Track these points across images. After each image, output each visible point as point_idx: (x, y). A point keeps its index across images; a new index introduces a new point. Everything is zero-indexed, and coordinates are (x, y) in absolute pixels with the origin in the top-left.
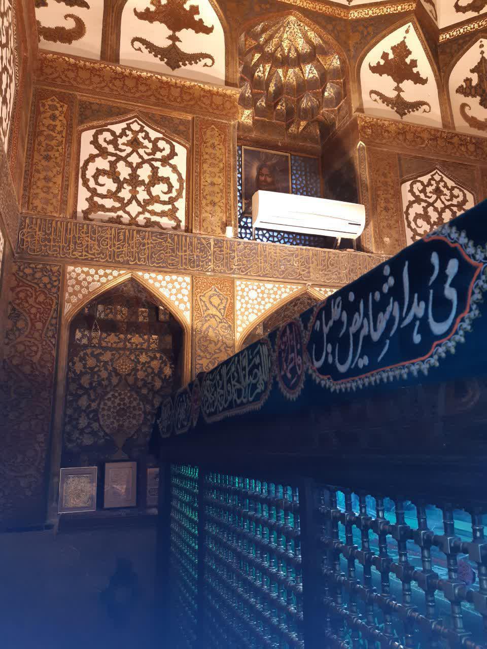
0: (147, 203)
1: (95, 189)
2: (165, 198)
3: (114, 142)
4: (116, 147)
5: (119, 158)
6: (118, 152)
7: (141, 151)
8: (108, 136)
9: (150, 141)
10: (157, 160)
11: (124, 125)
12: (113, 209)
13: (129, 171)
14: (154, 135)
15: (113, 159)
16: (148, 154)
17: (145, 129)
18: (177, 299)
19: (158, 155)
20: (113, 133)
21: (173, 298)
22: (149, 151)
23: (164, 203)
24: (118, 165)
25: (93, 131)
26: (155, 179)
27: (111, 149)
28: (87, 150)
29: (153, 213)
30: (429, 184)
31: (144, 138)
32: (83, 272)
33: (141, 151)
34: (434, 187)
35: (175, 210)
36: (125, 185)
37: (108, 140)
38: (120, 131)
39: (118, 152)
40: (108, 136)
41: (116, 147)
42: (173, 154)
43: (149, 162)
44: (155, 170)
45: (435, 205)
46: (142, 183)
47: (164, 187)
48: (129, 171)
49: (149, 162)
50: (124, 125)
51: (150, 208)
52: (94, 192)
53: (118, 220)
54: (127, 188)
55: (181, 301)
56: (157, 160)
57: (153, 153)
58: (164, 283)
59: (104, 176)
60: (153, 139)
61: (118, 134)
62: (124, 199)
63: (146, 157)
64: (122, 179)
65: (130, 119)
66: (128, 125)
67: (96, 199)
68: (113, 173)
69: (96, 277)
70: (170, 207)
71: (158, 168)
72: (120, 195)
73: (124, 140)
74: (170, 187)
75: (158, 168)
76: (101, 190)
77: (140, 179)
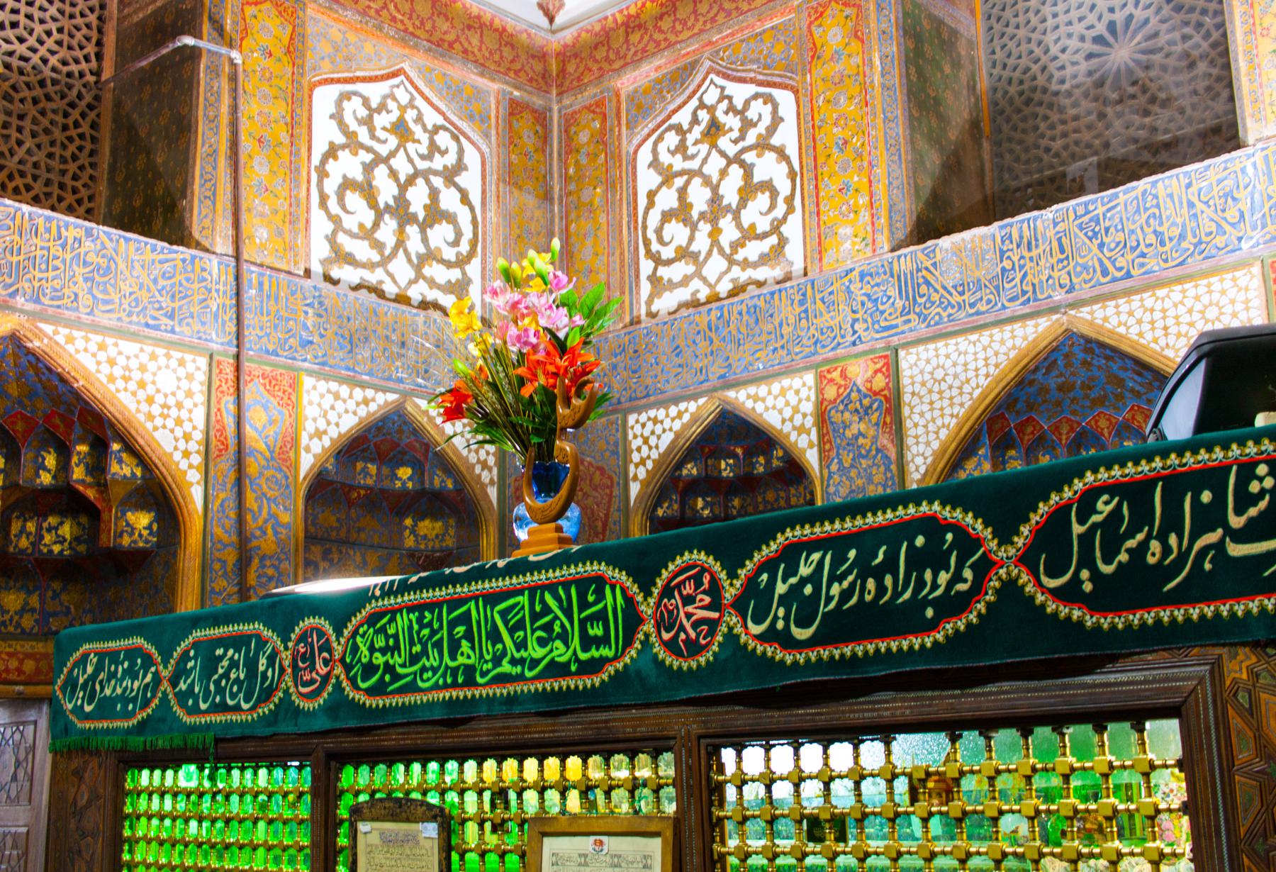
1: (658, 252)
3: (681, 149)
5: (691, 174)
8: (672, 139)
9: (736, 112)
11: (694, 103)
12: (685, 281)
13: (707, 193)
14: (740, 92)
15: (679, 182)
16: (735, 142)
17: (726, 93)
18: (794, 428)
20: (678, 129)
21: (787, 428)
22: (735, 134)
24: (690, 189)
25: (649, 144)
26: (749, 190)
28: (647, 179)
30: (382, 107)
31: (726, 113)
32: (649, 419)
33: (724, 143)
34: (394, 116)
36: (701, 225)
37: (672, 148)
38: (689, 118)
43: (737, 160)
44: (748, 170)
45: (393, 162)
46: (728, 208)
50: (694, 103)
52: (658, 261)
53: (694, 304)
54: (705, 228)
55: (801, 430)
58: (770, 401)
59: (670, 221)
60: (740, 107)
61: (686, 127)
65: (699, 86)
66: (701, 99)
68: (682, 212)
69: (667, 424)
71: (753, 165)
72: (694, 248)
74: (774, 193)
75: (753, 165)
77: (725, 202)
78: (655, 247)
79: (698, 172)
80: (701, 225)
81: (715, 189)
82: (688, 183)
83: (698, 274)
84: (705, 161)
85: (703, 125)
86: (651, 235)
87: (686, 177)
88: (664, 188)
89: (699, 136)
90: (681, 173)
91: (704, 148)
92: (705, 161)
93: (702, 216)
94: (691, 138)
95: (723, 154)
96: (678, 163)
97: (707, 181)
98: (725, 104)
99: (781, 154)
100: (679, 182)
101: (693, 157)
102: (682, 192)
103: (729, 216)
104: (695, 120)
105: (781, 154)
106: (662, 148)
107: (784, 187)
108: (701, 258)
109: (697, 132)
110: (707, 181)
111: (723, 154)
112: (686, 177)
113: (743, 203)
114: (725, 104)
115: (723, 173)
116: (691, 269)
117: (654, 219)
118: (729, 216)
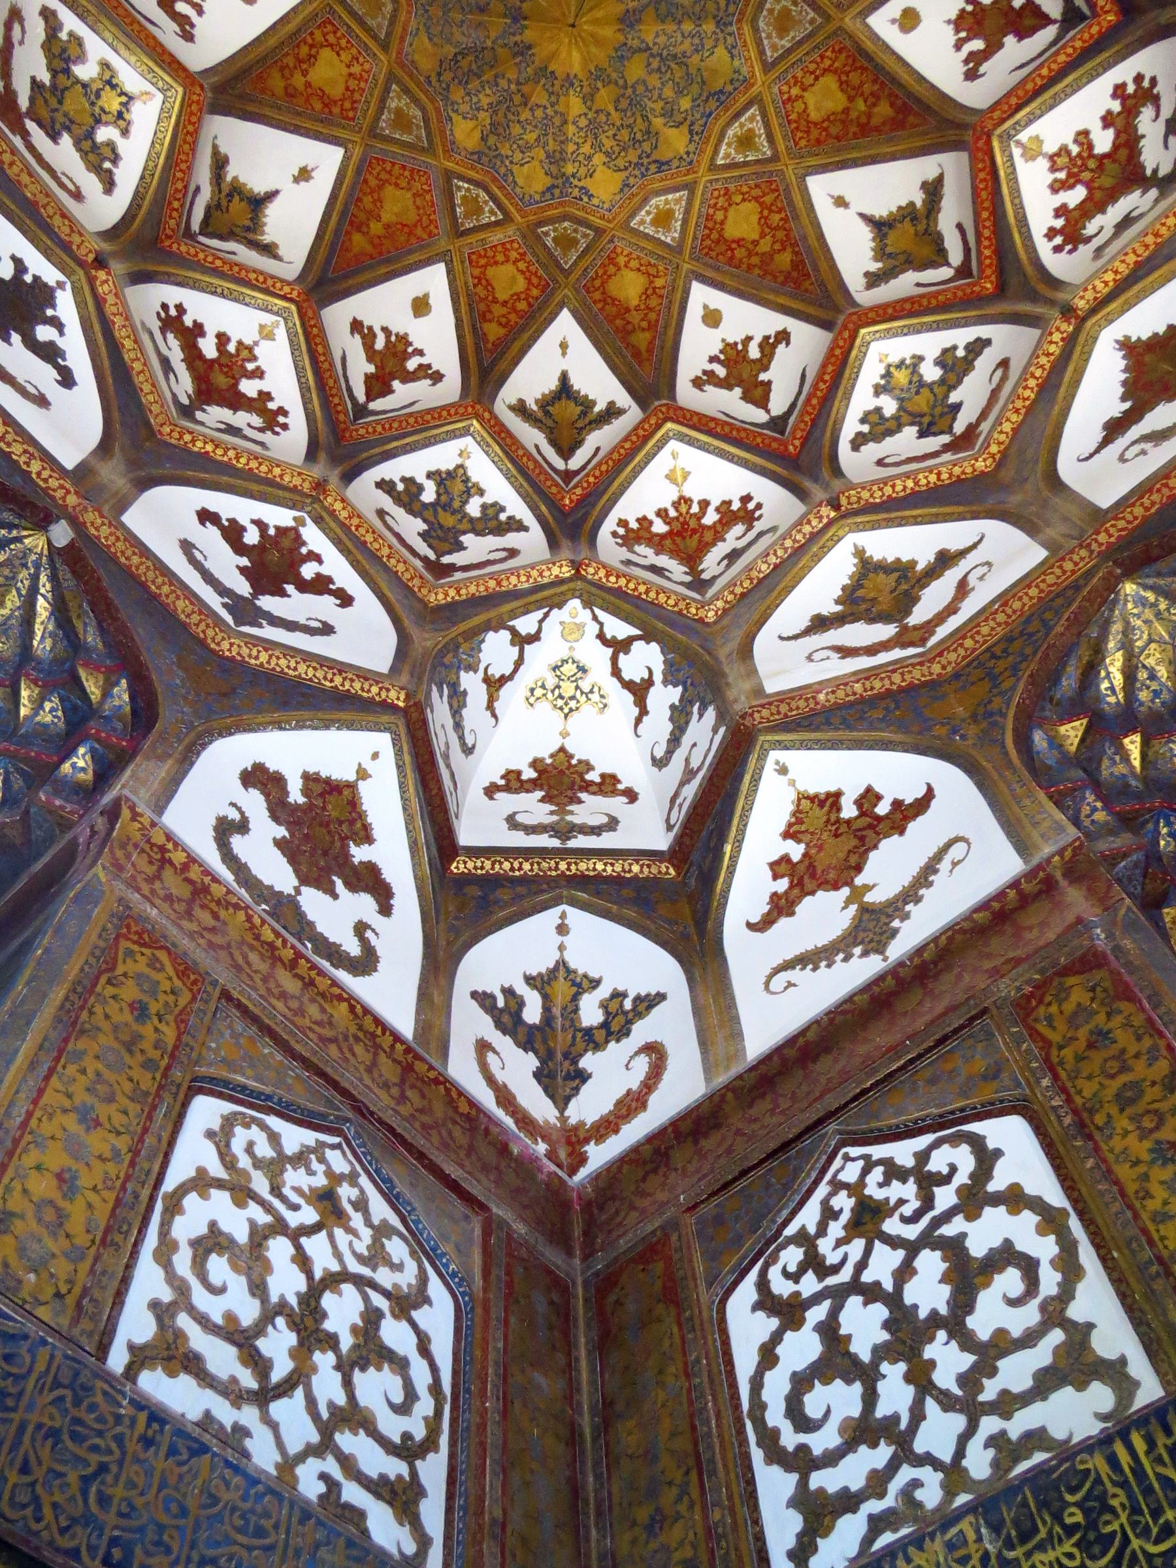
0: (970, 1380)
2: (1029, 1315)
4: (823, 1270)
5: (839, 1295)
6: (831, 1281)
7: (892, 1226)
10: (947, 1216)
12: (878, 1482)
13: (879, 1311)
14: (903, 1152)
15: (817, 1314)
19: (945, 1197)
22: (913, 1205)
23: (1030, 1339)
24: (843, 1317)
27: (809, 1284)
29: (1007, 1404)
33: (892, 1226)
35: (1080, 1334)
36: (885, 1367)
39: (831, 1281)
40: (792, 1256)
41: (823, 1270)
42: (986, 1159)
43: (928, 1240)
44: (954, 1248)
46: (935, 1320)
47: (1010, 1280)
48: (879, 1311)
49: (928, 1240)
51: (990, 1391)
56: (947, 1216)
57: (928, 1202)
62: (896, 1418)
63: (911, 1232)
64: (865, 1356)
67: (817, 1480)
70: (1056, 1336)
73: (836, 1229)
74: (1029, 1267)
76: (823, 1441)
77: (923, 1314)
78: (790, 1439)
79: (855, 1286)
80: (885, 1367)
81: (894, 1300)
82: (834, 1313)
83: (905, 1454)
84: (862, 1265)
85: (845, 1217)
86: (775, 1416)
87: (826, 1304)
88: (789, 1336)
89: (842, 1233)
90: (816, 1299)
91: (856, 1248)
92: (862, 1265)
93: (882, 1352)
94: (825, 1246)
95: (894, 1242)
96: (809, 1284)
97: (872, 1293)
98: (877, 1174)
99: (1015, 1199)
100: (817, 1314)
101: (836, 1269)
102: (829, 1331)
103: (942, 1335)
104: (829, 1214)
105: (1015, 1199)
106: (774, 1273)
107: (1045, 1249)
108: (903, 1425)
109: (836, 1229)
110: (872, 1293)
111: (894, 1242)
112: (826, 1304)
113: (963, 1301)
114: (877, 1174)
115: (905, 1272)
116: (883, 1454)
117: (776, 1387)
118: (942, 1335)
